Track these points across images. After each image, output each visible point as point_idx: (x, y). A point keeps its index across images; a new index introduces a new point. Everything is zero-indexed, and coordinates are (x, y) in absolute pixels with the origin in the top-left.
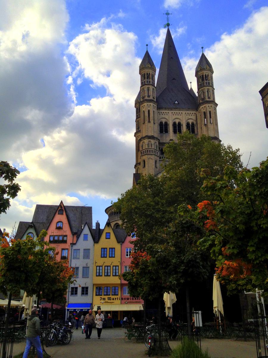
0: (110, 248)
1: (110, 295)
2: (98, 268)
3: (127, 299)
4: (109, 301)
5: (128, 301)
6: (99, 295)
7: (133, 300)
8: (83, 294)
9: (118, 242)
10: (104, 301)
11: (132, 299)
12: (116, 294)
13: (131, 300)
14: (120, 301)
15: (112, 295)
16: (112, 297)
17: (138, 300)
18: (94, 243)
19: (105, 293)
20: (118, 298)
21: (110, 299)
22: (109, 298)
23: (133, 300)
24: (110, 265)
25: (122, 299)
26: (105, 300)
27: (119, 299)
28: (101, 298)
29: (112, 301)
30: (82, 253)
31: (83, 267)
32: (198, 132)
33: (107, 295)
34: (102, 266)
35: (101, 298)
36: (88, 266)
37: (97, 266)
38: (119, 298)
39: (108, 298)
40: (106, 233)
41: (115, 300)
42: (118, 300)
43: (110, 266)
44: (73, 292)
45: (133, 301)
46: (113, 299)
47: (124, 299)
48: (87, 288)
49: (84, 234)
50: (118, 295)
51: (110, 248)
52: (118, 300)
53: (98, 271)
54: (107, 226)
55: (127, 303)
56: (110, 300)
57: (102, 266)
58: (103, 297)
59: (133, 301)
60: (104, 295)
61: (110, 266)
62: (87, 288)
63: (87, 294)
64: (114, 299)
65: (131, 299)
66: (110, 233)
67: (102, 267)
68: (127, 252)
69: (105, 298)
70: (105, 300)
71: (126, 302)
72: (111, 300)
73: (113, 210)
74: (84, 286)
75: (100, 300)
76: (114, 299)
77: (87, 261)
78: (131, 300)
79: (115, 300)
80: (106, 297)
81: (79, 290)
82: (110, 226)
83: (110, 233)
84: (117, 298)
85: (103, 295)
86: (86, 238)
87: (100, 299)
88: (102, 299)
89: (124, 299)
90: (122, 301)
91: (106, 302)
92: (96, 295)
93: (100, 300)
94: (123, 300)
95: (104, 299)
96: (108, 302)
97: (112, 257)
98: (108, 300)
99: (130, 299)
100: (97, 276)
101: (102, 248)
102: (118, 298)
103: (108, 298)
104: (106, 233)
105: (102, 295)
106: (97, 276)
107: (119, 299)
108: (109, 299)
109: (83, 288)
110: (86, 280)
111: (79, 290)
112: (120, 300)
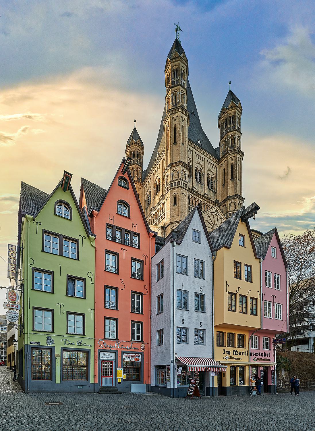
3: (256, 355)
4: (235, 356)
10: (229, 356)
11: (262, 356)
13: (260, 356)
17: (268, 356)
20: (245, 353)
26: (230, 354)
28: (224, 350)
29: (238, 356)
32: (217, 190)
35: (224, 350)
38: (247, 353)
41: (243, 355)
42: (245, 355)
52: (245, 355)
56: (235, 354)
58: (227, 349)
70: (230, 354)
71: (255, 360)
72: (237, 354)
78: (260, 356)
79: (243, 355)
80: (231, 349)
84: (244, 352)
88: (226, 352)
91: (231, 358)
93: (224, 354)
95: (228, 353)
98: (234, 354)
102: (245, 353)
107: (246, 354)
108: (235, 352)
112: (247, 355)
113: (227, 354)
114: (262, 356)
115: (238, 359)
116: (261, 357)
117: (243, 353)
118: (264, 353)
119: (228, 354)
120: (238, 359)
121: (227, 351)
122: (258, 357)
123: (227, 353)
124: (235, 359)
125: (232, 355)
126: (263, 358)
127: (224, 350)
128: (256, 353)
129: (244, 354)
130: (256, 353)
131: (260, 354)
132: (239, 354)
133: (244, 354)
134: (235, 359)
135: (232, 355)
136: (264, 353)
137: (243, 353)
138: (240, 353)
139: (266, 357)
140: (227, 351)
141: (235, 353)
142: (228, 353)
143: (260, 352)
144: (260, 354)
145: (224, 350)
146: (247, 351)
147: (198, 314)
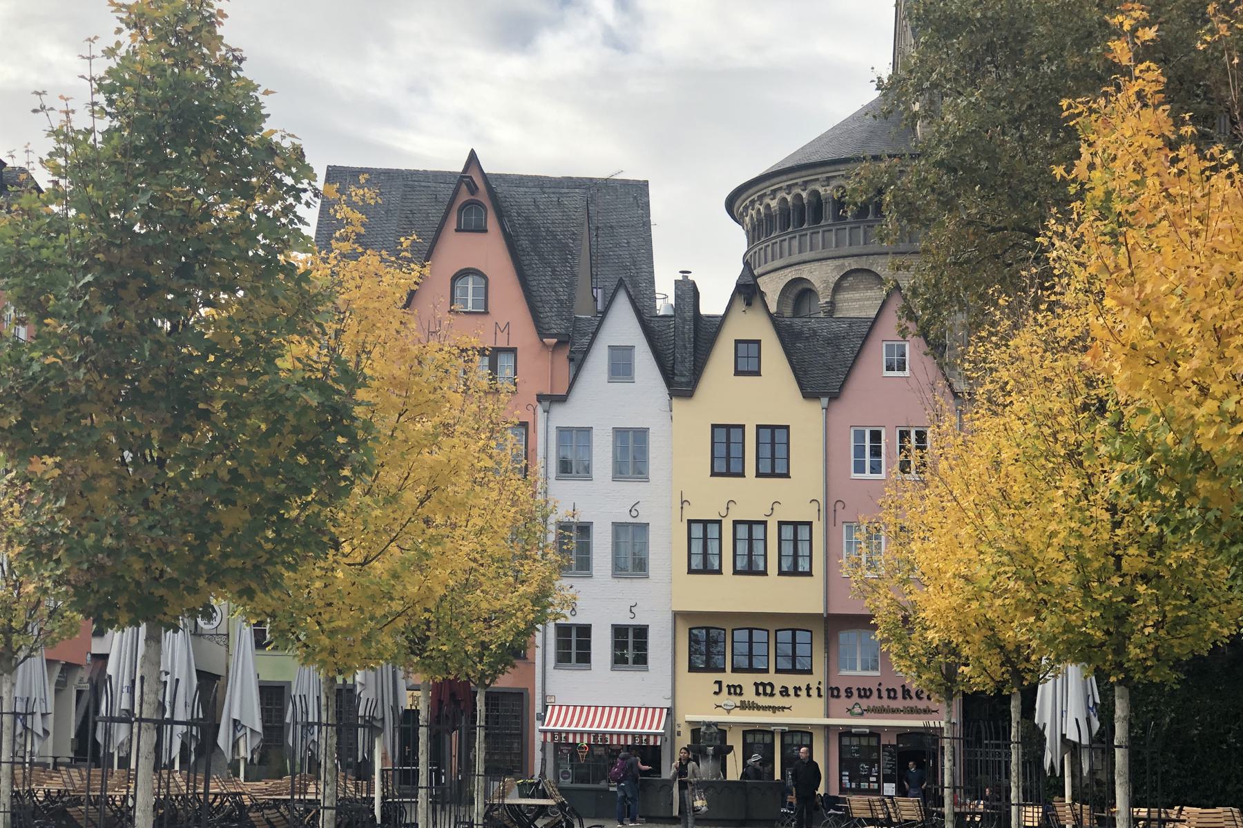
0: (759, 427)
1: (766, 671)
2: (697, 531)
3: (860, 696)
4: (763, 701)
5: (865, 703)
6: (710, 668)
7: (895, 698)
8: (619, 660)
9: (809, 392)
10: (737, 700)
11: (889, 697)
12: (798, 667)
13: (880, 697)
14: (822, 700)
15: (778, 671)
16: (780, 681)
17: (920, 698)
18: (671, 396)
19: (744, 662)
20: (808, 688)
21: (769, 690)
22: (764, 685)
23: (895, 698)
24: (764, 519)
25: (833, 692)
26: (741, 694)
27: (814, 692)
28: (719, 683)
29: (778, 701)
30: (602, 454)
31: (618, 527)
33: (751, 669)
34: (719, 522)
35: (719, 683)
36: (641, 520)
37: (690, 522)
38: (819, 689)
39: (756, 684)
40: (737, 342)
41: (797, 695)
42: (809, 695)
43: (765, 523)
44: (570, 648)
45: (893, 704)
46: (785, 692)
47: (843, 694)
48: (641, 632)
49: (612, 348)
50: (810, 672)
51: (759, 427)
52: (809, 695)
53: (697, 547)
54: (740, 305)
55: (861, 714)
56: (765, 694)
57: (719, 522)
58: (729, 678)
59: (893, 704)
60: (734, 670)
61: (765, 523)
62: (641, 632)
63: (641, 660)
64: (791, 692)
65: (885, 694)
66: (758, 342)
67: (716, 526)
68: (859, 451)
69: (740, 686)
70: (741, 694)
71: (857, 710)
72: (772, 695)
73: (774, 204)
74: (625, 620)
75: (716, 693)
76: (791, 692)
77: (631, 490)
78: (880, 697)
81: (601, 645)
82: (757, 303)
83: (758, 342)
84: (804, 688)
85: (728, 667)
86: (621, 367)
87: (716, 688)
88: (725, 690)
89: (843, 694)
90: (833, 701)
91: (744, 706)
92: (692, 668)
93: (716, 693)
94: (838, 696)
95: (735, 690)
96: (759, 708)
97: (773, 475)
98: (758, 694)
99: (875, 693)
100: (691, 571)
101: (714, 426)
102: (808, 688)
103: (756, 684)
104: (737, 342)
105: (723, 670)
106: (691, 571)
107: (814, 692)
109: (619, 632)
110: (631, 589)
111: (601, 645)
112: (820, 696)
113: (730, 693)
114: (889, 697)
115: (774, 709)
116: (886, 702)
117: (797, 689)
118: (903, 686)
119: (735, 693)
120: (774, 709)
121: (728, 686)
122: (874, 701)
123: (729, 690)
124: (765, 708)
125: (749, 695)
126: (899, 703)
127: (716, 682)
128: (859, 689)
129: (803, 693)
130: (859, 689)
131: (879, 690)
132: (781, 692)
133: (803, 693)
134: (765, 708)
135: (749, 695)
136: (903, 686)
137: (797, 689)
138: (786, 689)
139: (914, 703)
140: (728, 686)
141: (764, 690)
142: (735, 690)
143: (880, 684)
144: (879, 690)
145: (716, 682)
146: (820, 683)
147: (624, 584)
